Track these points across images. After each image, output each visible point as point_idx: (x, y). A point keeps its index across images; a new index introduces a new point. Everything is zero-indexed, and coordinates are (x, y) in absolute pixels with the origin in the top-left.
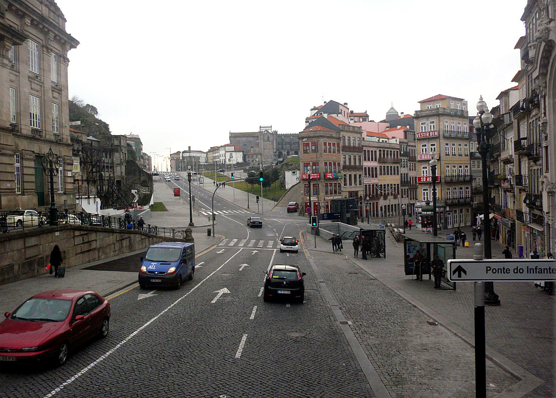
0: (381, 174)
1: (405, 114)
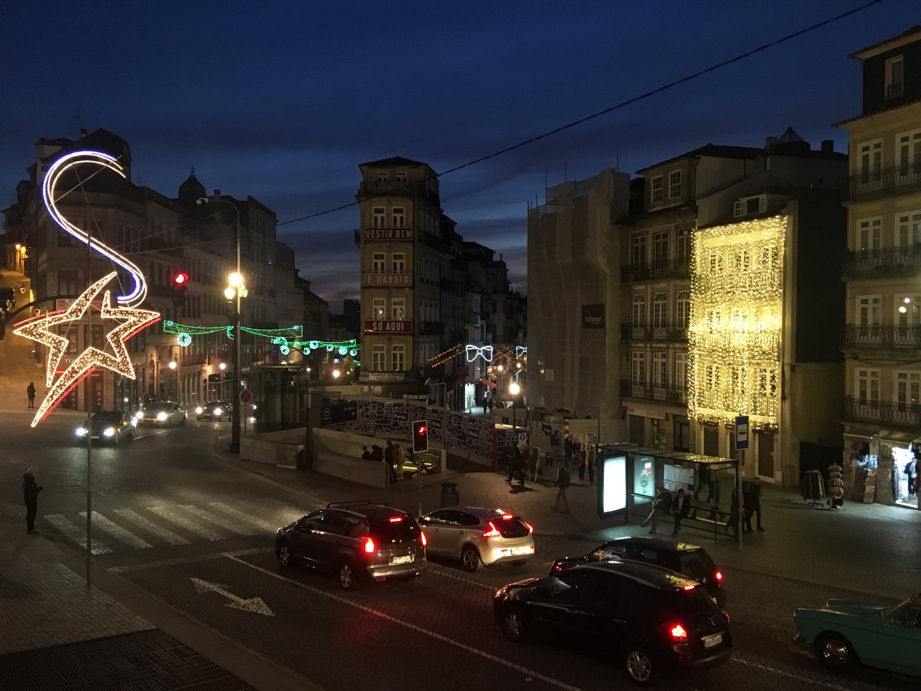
0: (205, 312)
1: (222, 194)
